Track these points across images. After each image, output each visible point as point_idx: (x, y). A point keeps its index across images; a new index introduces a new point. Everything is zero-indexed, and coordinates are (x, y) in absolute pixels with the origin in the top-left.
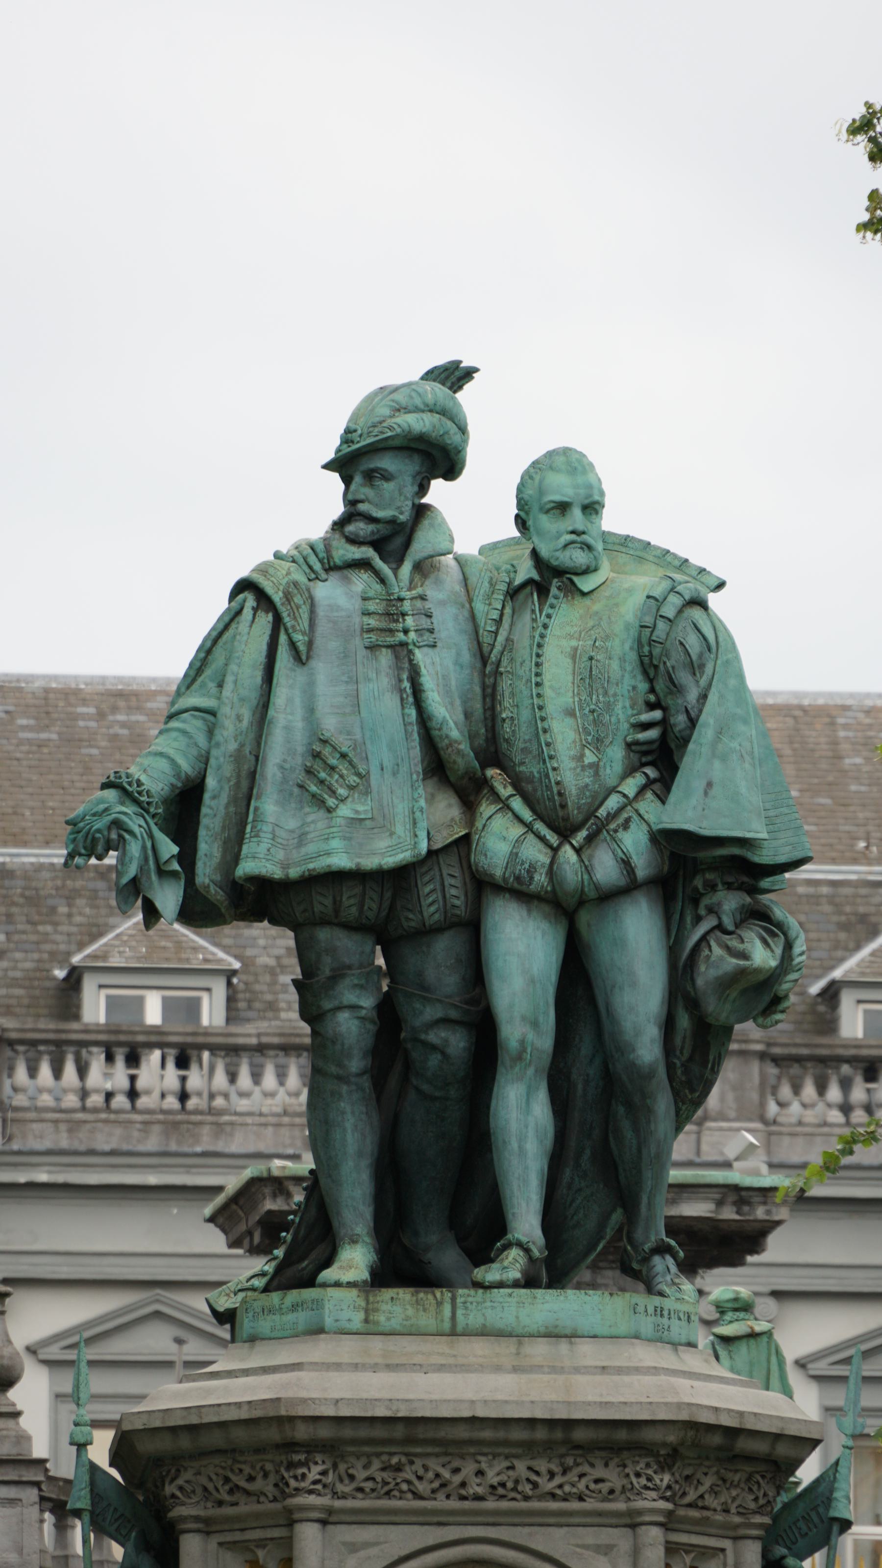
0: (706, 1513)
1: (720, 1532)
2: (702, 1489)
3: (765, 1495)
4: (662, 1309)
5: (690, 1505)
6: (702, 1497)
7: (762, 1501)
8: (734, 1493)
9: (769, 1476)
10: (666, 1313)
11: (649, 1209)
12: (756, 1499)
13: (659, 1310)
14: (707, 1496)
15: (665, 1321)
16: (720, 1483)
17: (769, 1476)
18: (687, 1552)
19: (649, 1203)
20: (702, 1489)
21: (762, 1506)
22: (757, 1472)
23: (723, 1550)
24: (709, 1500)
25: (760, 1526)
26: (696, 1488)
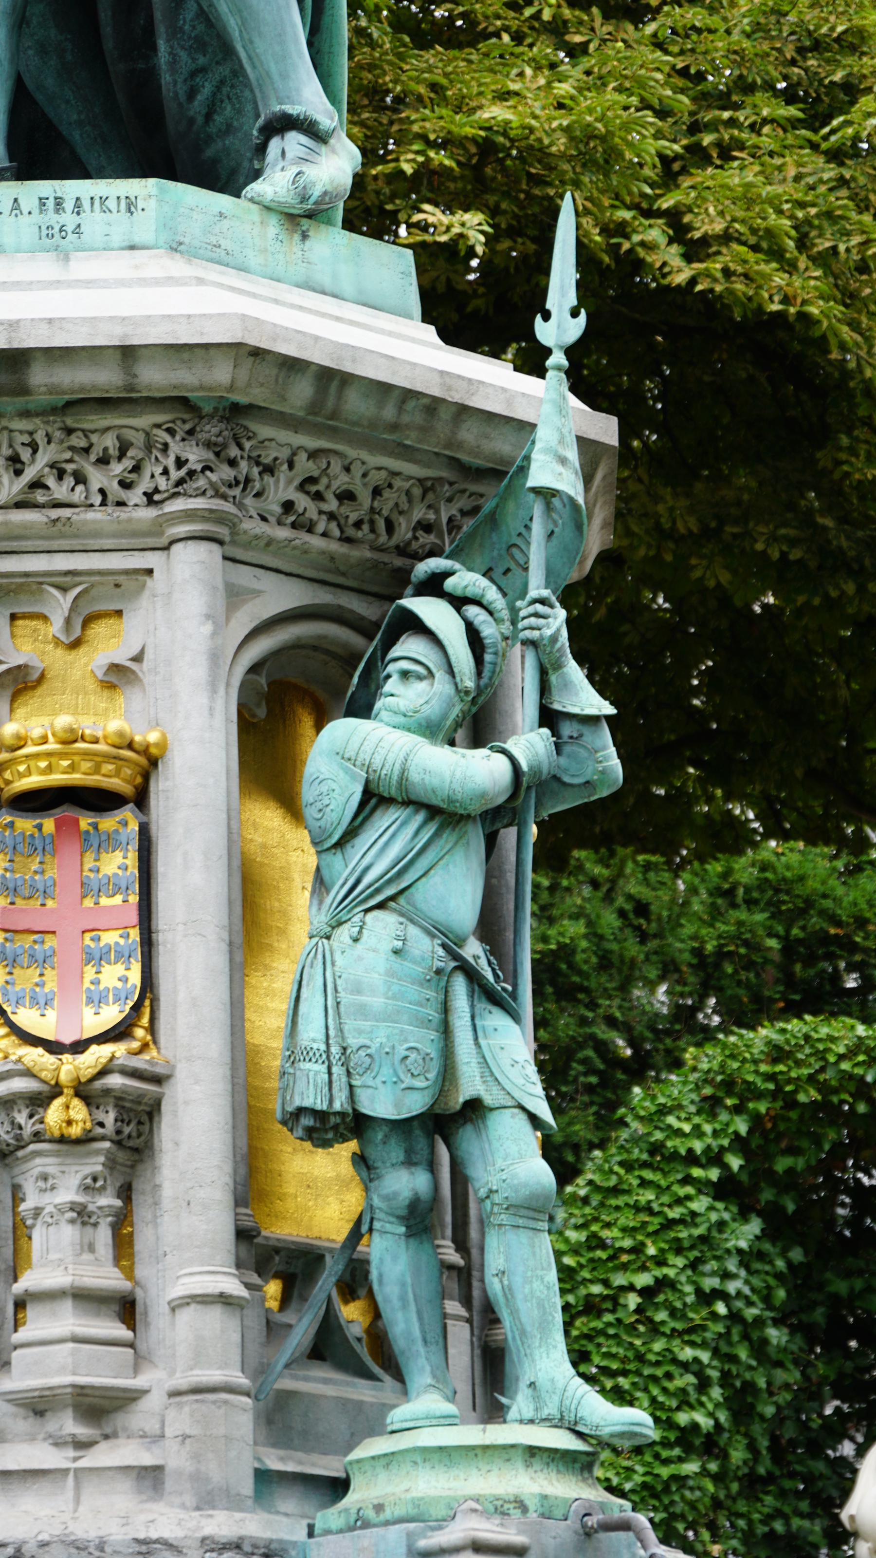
0: (55, 513)
1: (124, 543)
2: (30, 474)
3: (180, 463)
4: (59, 203)
5: (19, 505)
6: (37, 484)
7: (175, 475)
8: (117, 468)
9: (181, 429)
10: (69, 205)
11: (254, 67)
12: (166, 472)
13: (50, 204)
14: (51, 482)
15: (69, 219)
16: (68, 455)
17: (181, 429)
18: (64, 589)
19: (250, 58)
20: (30, 474)
21: (180, 482)
22: (158, 426)
23: (150, 572)
24: (60, 490)
25: (189, 516)
26: (18, 473)
